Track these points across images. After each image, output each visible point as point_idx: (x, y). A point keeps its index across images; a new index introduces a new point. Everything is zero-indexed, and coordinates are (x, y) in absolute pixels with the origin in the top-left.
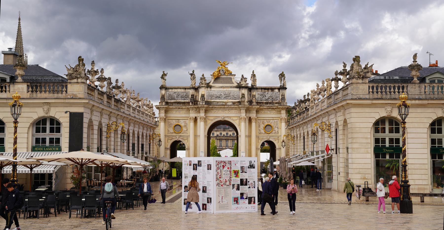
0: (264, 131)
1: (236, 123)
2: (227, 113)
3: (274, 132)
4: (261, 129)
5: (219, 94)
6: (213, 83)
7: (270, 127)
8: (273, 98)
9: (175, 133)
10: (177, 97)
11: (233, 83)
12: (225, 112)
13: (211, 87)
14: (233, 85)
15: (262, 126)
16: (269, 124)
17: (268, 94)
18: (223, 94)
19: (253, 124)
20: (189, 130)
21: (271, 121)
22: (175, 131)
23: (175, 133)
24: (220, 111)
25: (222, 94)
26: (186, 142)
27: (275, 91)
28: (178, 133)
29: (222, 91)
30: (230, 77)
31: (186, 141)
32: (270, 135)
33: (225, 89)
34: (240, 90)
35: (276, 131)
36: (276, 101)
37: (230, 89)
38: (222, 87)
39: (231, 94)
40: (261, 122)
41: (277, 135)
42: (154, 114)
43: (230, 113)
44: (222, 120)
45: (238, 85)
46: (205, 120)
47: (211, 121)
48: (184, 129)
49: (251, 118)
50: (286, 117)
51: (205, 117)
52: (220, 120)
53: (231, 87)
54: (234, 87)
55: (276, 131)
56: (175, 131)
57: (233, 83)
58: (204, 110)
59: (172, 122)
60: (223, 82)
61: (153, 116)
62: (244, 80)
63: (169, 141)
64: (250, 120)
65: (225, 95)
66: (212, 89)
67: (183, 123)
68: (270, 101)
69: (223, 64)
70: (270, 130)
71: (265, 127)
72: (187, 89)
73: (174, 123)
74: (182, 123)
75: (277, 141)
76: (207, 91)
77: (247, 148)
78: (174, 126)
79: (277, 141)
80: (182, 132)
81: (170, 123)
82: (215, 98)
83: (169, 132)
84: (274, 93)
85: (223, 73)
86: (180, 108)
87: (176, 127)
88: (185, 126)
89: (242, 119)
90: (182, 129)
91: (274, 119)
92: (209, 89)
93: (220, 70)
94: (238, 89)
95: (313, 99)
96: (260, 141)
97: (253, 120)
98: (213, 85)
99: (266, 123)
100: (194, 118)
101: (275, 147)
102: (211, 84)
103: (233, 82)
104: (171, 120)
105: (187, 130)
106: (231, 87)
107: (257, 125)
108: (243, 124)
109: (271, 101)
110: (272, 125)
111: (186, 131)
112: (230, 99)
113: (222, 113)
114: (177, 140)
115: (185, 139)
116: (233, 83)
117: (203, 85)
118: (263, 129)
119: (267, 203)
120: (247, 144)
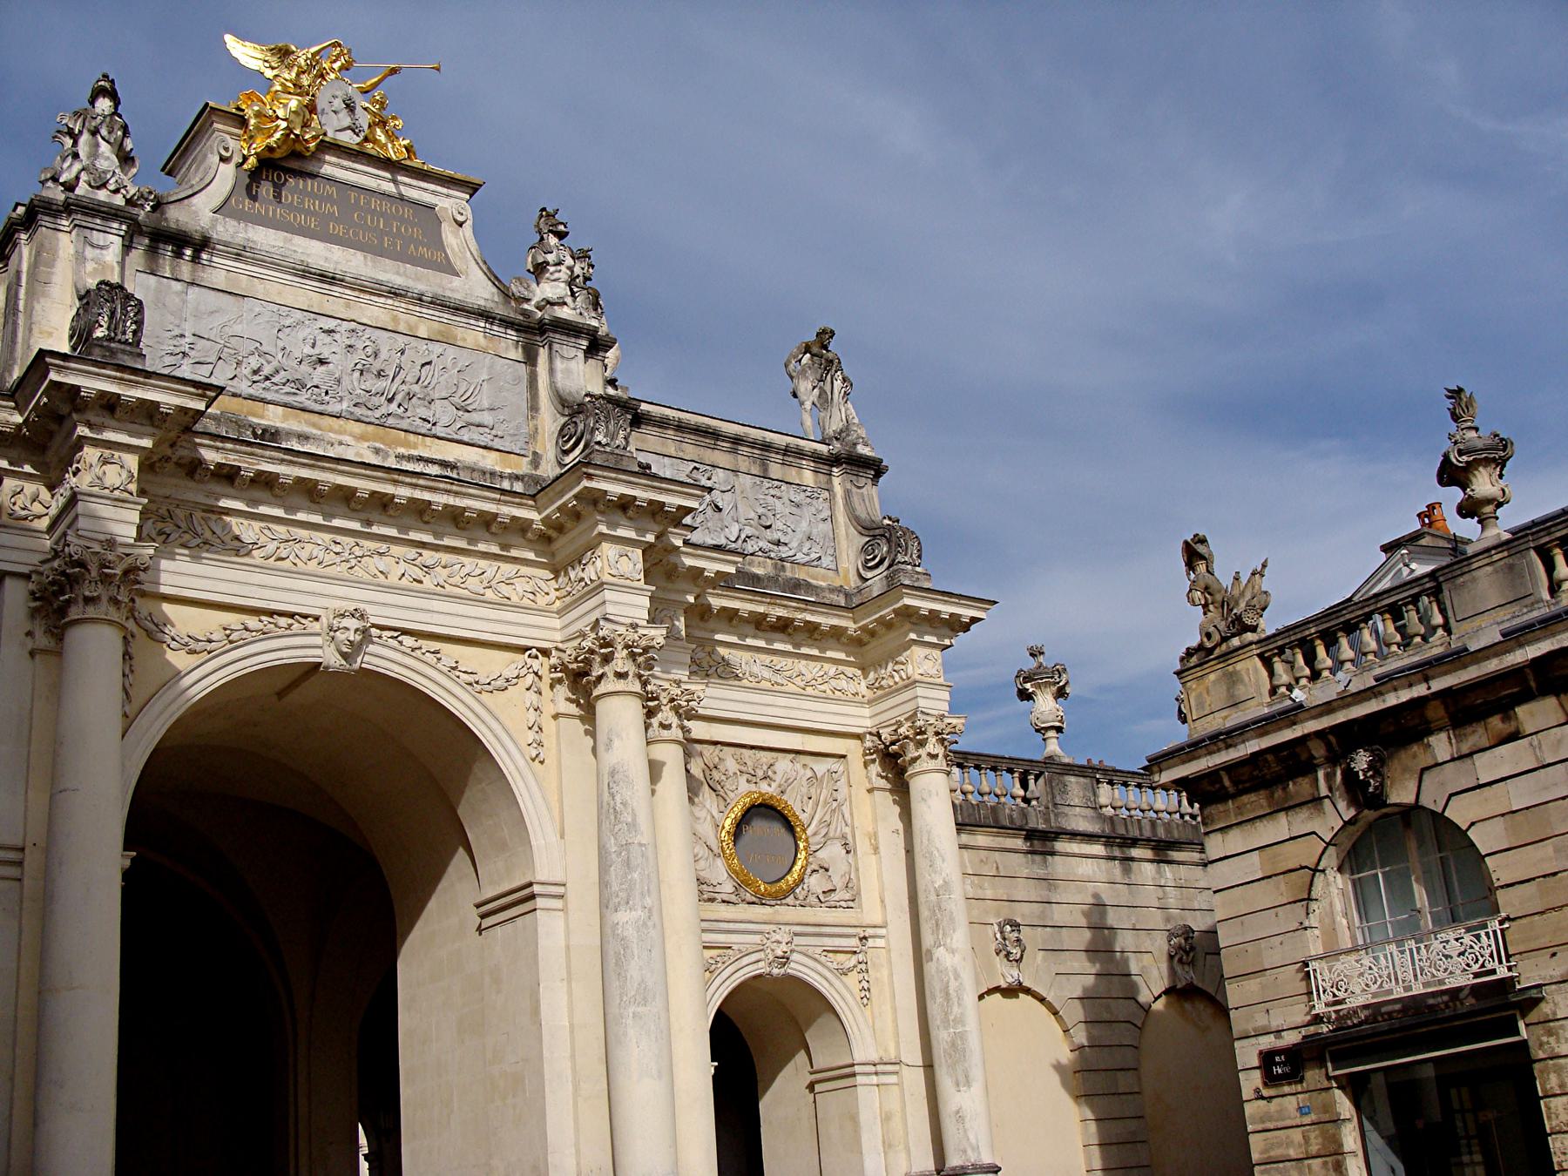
0: (733, 873)
2: (393, 579)
3: (815, 883)
7: (777, 829)
8: (778, 543)
11: (450, 269)
14: (456, 281)
21: (784, 764)
29: (331, 324)
30: (427, 198)
32: (785, 912)
35: (838, 882)
43: (428, 583)
44: (331, 658)
52: (311, 656)
57: (450, 269)
58: (132, 461)
60: (340, 230)
66: (219, 270)
79: (853, 979)
85: (353, 129)
89: (621, 654)
94: (509, 345)
98: (226, 230)
99: (743, 786)
103: (458, 264)
110: (794, 803)
113: (330, 571)
118: (714, 845)
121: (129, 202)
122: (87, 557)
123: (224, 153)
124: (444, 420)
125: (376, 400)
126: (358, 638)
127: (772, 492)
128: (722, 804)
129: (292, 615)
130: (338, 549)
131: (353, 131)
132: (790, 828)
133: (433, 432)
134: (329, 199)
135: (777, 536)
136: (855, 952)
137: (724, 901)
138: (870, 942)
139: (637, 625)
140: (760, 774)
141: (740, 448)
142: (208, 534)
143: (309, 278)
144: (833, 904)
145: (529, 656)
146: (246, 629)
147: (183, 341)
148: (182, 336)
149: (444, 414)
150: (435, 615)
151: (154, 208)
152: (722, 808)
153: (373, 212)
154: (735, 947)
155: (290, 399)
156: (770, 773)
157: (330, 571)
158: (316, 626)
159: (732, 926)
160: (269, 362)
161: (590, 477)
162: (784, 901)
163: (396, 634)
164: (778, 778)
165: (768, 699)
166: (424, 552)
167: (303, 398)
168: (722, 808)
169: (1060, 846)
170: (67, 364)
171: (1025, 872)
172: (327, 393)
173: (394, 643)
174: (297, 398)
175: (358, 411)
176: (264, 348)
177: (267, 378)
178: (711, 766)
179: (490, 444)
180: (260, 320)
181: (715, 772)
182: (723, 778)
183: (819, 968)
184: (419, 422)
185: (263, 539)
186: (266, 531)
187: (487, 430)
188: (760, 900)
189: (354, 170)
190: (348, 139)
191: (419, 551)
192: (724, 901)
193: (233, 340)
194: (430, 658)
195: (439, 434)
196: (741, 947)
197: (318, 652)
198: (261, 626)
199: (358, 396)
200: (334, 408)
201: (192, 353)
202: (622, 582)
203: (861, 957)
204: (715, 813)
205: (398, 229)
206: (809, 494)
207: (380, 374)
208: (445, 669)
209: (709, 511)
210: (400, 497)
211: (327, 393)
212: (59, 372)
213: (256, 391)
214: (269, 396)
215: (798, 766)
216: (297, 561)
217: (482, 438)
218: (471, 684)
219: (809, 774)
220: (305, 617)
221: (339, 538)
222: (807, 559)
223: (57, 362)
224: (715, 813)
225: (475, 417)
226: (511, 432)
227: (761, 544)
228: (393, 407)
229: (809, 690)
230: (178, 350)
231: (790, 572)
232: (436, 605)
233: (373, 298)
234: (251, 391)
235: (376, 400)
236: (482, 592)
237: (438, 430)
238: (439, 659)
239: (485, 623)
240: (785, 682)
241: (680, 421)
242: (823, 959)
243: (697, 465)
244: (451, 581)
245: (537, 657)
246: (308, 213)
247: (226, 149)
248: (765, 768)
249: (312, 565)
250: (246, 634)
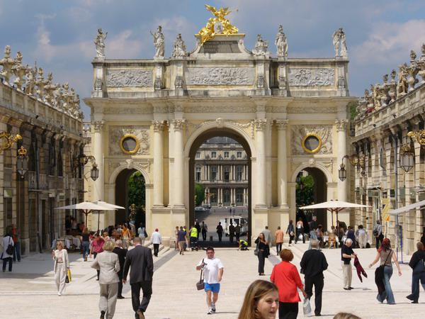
1: (247, 133)
3: (323, 150)
4: (297, 146)
7: (316, 140)
9: (124, 153)
13: (194, 62)
15: (299, 139)
19: (283, 137)
20: (151, 147)
23: (124, 153)
31: (147, 170)
32: (316, 156)
42: (81, 116)
44: (217, 126)
45: (250, 55)
46: (184, 127)
48: (143, 146)
50: (347, 121)
51: (183, 121)
52: (215, 126)
55: (328, 149)
61: (80, 120)
64: (275, 126)
65: (224, 76)
69: (219, 13)
70: (315, 146)
74: (138, 134)
77: (270, 182)
78: (122, 139)
79: (330, 169)
81: (113, 134)
83: (113, 153)
86: (134, 104)
88: (145, 140)
90: (139, 147)
93: (213, 26)
95: (402, 84)
96: (294, 168)
101: (327, 181)
102: (196, 55)
105: (148, 148)
107: (289, 137)
108: (260, 136)
110: (319, 136)
116: (241, 52)
120: (270, 175)
167: (213, 83)
190: (219, 34)
231: (322, 89)
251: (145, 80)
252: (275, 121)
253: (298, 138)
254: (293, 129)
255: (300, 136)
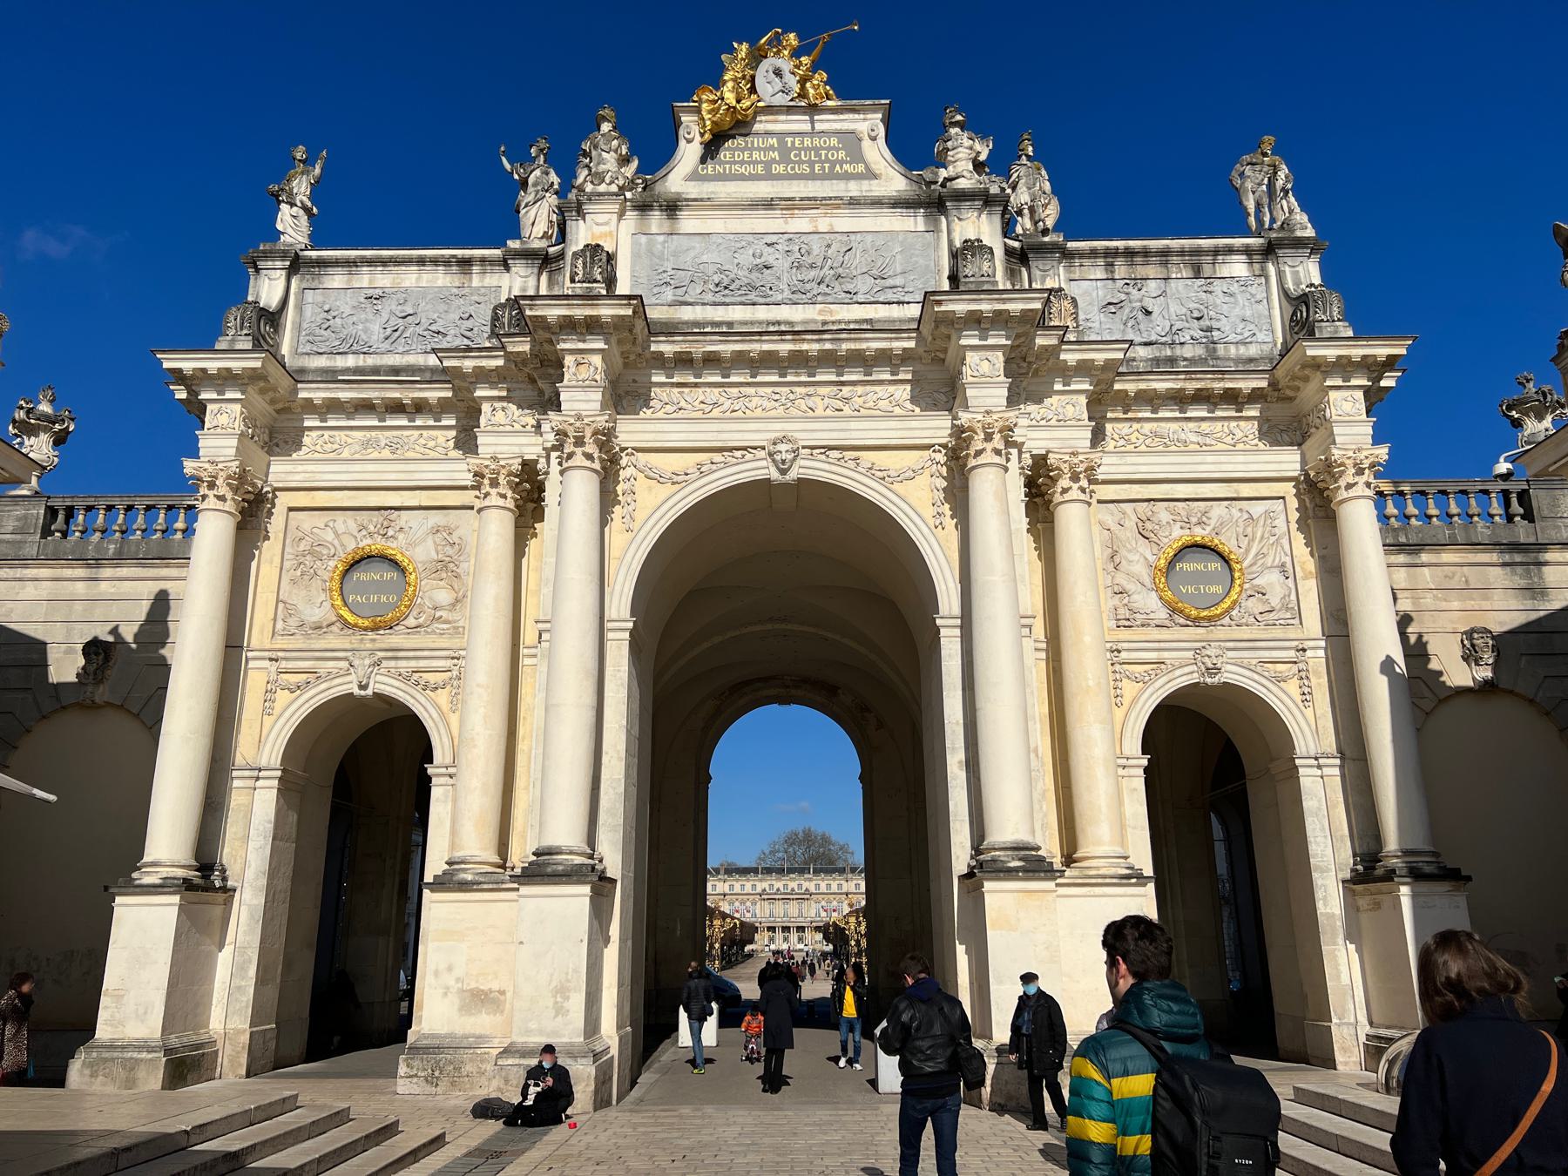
2: (819, 412)
5: (746, 258)
6: (694, 177)
7: (1215, 565)
8: (1210, 329)
9: (346, 624)
10: (393, 335)
11: (871, 175)
12: (802, 404)
15: (1141, 559)
16: (1200, 534)
17: (1163, 294)
18: (781, 264)
21: (1218, 510)
22: (345, 613)
24: (756, 401)
25: (770, 256)
26: (445, 706)
27: (1224, 271)
28: (375, 629)
29: (774, 238)
31: (442, 697)
32: (1219, 633)
33: (800, 223)
34: (935, 230)
35: (1275, 602)
36: (1242, 349)
37: (845, 221)
38: (769, 204)
39: (857, 261)
40: (1131, 523)
41: (1292, 633)
43: (847, 411)
44: (774, 475)
47: (668, 489)
49: (1052, 459)
52: (760, 474)
53: (854, 202)
54: (877, 203)
56: (345, 613)
57: (871, 175)
58: (597, 360)
59: (329, 536)
60: (779, 169)
62: (968, 143)
63: (283, 697)
66: (688, 222)
67: (430, 542)
68: (1188, 351)
70: (1218, 589)
71: (1171, 564)
72: (476, 269)
73: (348, 536)
75: (1293, 687)
76: (643, 239)
80: (411, 622)
82: (709, 297)
84: (1218, 287)
87: (359, 575)
88: (445, 567)
91: (1246, 490)
92: (656, 220)
96: (1129, 688)
97: (1064, 482)
98: (693, 190)
100: (516, 466)
104: (319, 519)
106: (854, 202)
109: (1200, 351)
110: (1228, 544)
111: (453, 605)
112: (851, 298)
113: (773, 413)
114: (356, 691)
115: (432, 678)
116: (875, 177)
117: (602, 188)
118: (1147, 581)
119: (898, 1057)
121: (621, 188)
122: (566, 426)
123: (687, 136)
124: (863, 289)
125: (808, 286)
126: (790, 456)
127: (1205, 288)
128: (1155, 548)
129: (745, 449)
130: (777, 397)
131: (783, 92)
132: (1225, 560)
133: (855, 300)
134: (772, 148)
135: (1205, 323)
136: (1295, 663)
137: (1157, 626)
138: (1309, 653)
139: (991, 412)
140: (1194, 520)
141: (1170, 258)
142: (683, 404)
143: (757, 210)
144: (1271, 622)
145: (934, 451)
146: (712, 463)
147: (665, 275)
148: (664, 272)
149: (863, 285)
150: (853, 432)
151: (644, 189)
152: (1155, 551)
153: (806, 149)
154: (1168, 662)
155: (743, 299)
156: (1204, 519)
157: (773, 413)
158: (762, 454)
159: (1162, 645)
160: (727, 276)
161: (939, 303)
162: (1218, 623)
163: (823, 451)
164: (1213, 523)
165: (1198, 458)
166: (843, 388)
168: (1155, 551)
169: (1549, 556)
170: (534, 302)
171: (1508, 584)
172: (771, 288)
173: (823, 457)
174: (749, 297)
175: (795, 297)
176: (724, 268)
177: (726, 288)
178: (1144, 518)
179: (902, 299)
180: (721, 248)
181: (1149, 525)
182: (1157, 527)
183: (1256, 677)
184: (844, 295)
185: (722, 400)
186: (724, 394)
187: (900, 289)
188: (1196, 621)
189: (776, 121)
191: (840, 388)
192: (1157, 626)
193: (701, 266)
194: (852, 464)
195: (860, 301)
196: (1173, 662)
197: (766, 471)
198: (723, 459)
199: (795, 285)
200: (779, 297)
201: (672, 282)
202: (984, 380)
203: (1301, 666)
204: (1151, 558)
205: (826, 155)
206: (1242, 283)
207: (812, 266)
208: (864, 471)
209: (1140, 316)
210: (812, 351)
211: (771, 288)
212: (531, 309)
213: (719, 298)
214: (727, 300)
215: (1235, 512)
216: (747, 411)
217: (895, 296)
218: (884, 479)
219: (1246, 516)
220: (755, 448)
221: (777, 389)
222: (1240, 337)
223: (527, 302)
224: (1151, 558)
225: (890, 282)
226: (921, 286)
227: (1192, 332)
228: (823, 288)
229: (1240, 446)
230: (662, 282)
232: (853, 425)
233: (805, 212)
234: (714, 299)
235: (808, 286)
236: (891, 409)
237: (861, 298)
238: (858, 464)
239: (894, 432)
240: (1213, 442)
241: (1108, 248)
242: (1259, 669)
243: (1128, 281)
244: (867, 405)
245: (940, 451)
246: (756, 162)
247: (689, 133)
248: (1199, 515)
249: (758, 412)
250: (714, 467)
251: (469, 324)
252: (1040, 462)
253: (1134, 557)
254: (1110, 521)
255: (1145, 549)
